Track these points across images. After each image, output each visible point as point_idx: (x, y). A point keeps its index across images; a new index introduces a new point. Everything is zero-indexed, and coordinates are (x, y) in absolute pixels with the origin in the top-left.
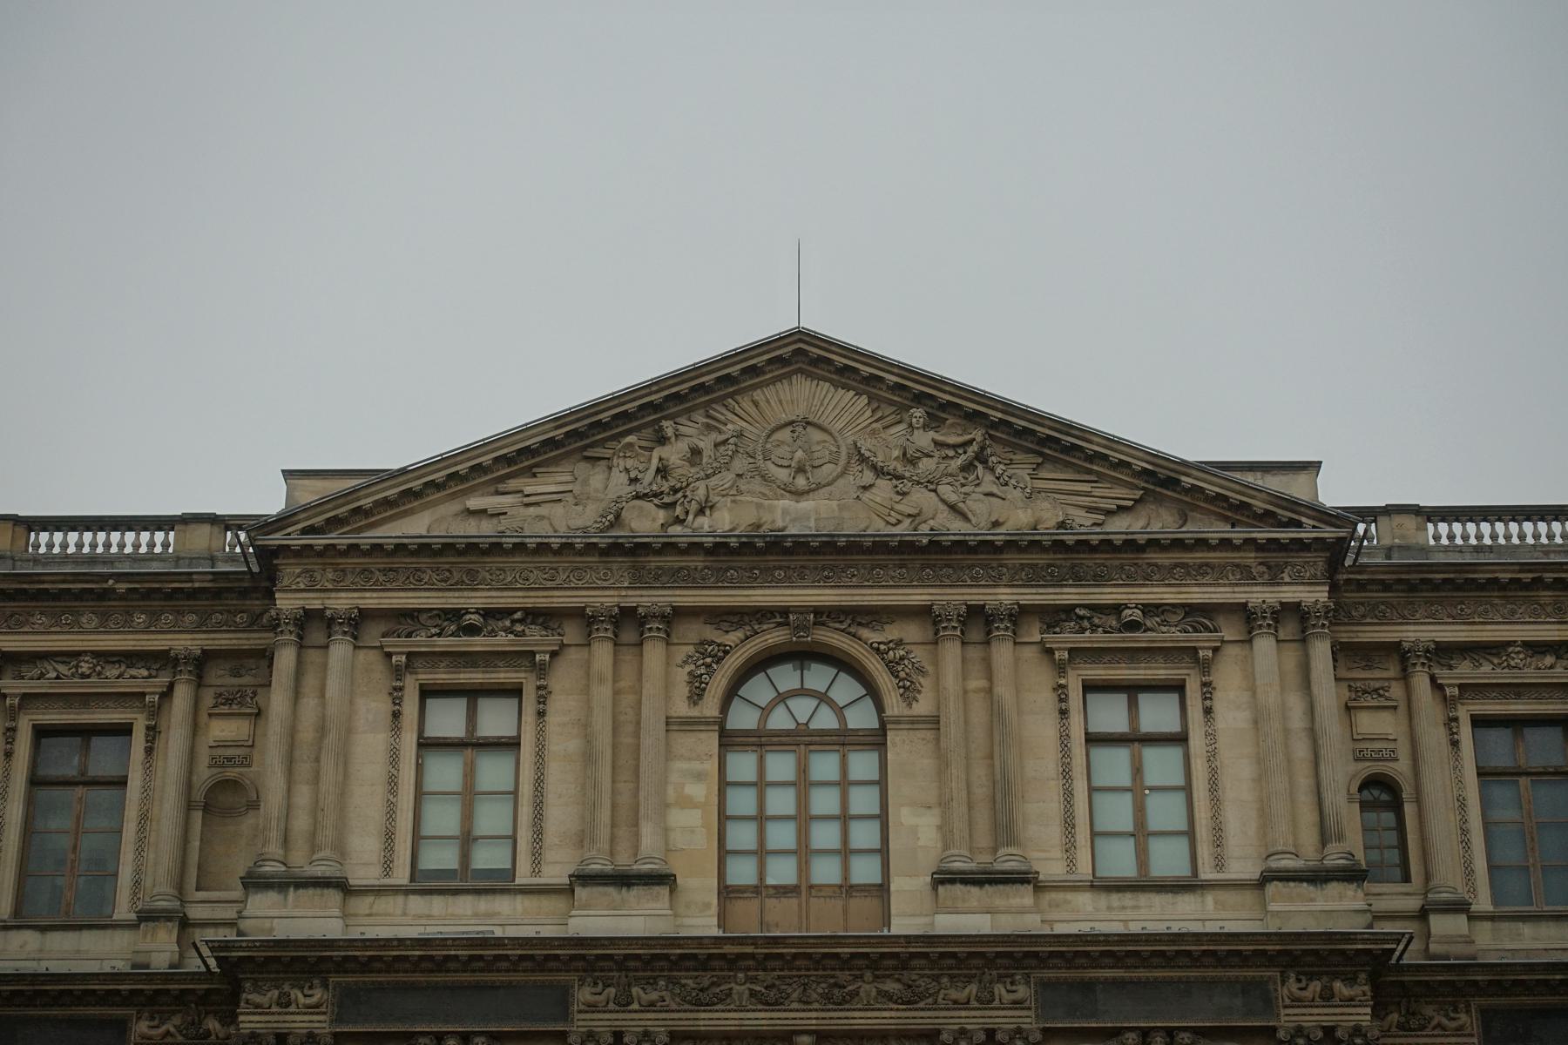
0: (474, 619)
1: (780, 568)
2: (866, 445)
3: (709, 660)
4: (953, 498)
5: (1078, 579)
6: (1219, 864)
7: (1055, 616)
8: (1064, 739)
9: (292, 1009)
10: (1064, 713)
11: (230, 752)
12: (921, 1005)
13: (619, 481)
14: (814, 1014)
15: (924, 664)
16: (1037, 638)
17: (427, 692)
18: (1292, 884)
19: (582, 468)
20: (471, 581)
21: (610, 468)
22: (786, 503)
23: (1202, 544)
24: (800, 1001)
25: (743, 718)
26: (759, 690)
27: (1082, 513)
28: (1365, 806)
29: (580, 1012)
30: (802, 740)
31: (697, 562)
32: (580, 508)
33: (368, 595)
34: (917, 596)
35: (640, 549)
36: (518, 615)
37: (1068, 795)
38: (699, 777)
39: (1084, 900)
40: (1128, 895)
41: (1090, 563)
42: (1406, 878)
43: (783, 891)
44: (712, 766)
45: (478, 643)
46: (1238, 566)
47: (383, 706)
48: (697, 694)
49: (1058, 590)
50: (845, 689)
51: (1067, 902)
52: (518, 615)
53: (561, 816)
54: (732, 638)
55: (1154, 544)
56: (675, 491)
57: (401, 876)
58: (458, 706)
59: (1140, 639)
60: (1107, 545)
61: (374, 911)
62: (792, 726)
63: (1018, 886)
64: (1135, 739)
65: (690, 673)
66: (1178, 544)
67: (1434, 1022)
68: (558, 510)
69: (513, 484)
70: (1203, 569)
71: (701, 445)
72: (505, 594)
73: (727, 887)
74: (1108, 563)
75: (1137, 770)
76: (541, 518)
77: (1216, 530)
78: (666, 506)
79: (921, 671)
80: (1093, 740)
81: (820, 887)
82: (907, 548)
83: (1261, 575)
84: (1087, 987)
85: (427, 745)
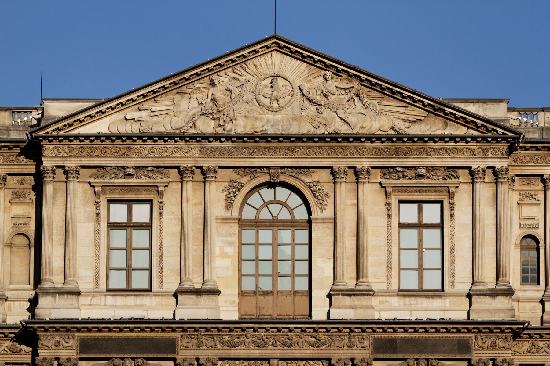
0: (131, 171)
1: (266, 148)
2: (305, 88)
3: (234, 190)
4: (343, 116)
5: (397, 153)
6: (453, 286)
7: (387, 171)
8: (389, 228)
9: (61, 347)
10: (389, 216)
11: (21, 220)
12: (324, 347)
13: (194, 103)
14: (279, 351)
15: (329, 192)
16: (379, 180)
17: (110, 201)
18: (482, 297)
19: (178, 97)
20: (129, 152)
21: (190, 98)
22: (270, 116)
23: (453, 138)
24: (272, 345)
25: (249, 214)
26: (255, 200)
27: (401, 122)
28: (522, 248)
29: (181, 350)
30: (274, 224)
31: (228, 144)
32: (176, 118)
33: (83, 159)
34: (326, 162)
35: (206, 138)
36: (150, 168)
37: (390, 254)
38: (231, 243)
39: (395, 301)
40: (413, 299)
41: (404, 147)
42: (538, 284)
43: (266, 293)
44: (235, 239)
45: (133, 181)
46: (469, 149)
47: (92, 209)
48: (229, 205)
49: (388, 160)
50: (295, 200)
51: (387, 301)
52: (150, 168)
53: (171, 260)
54: (245, 180)
55: (432, 138)
56: (220, 112)
57: (103, 287)
58: (123, 208)
59: (425, 182)
60: (411, 138)
61: (92, 303)
62: (271, 218)
63: (366, 297)
64: (420, 226)
65: (226, 196)
66: (442, 138)
67: (543, 350)
68: (168, 119)
69: (147, 105)
70: (454, 150)
71: (231, 88)
72: (144, 159)
73: (242, 291)
74: (411, 147)
75: (420, 241)
76: (158, 123)
77: (462, 131)
78: (214, 119)
79: (327, 195)
80: (402, 226)
81: (282, 292)
82: (322, 138)
83: (479, 153)
84: (393, 341)
85: (112, 226)
